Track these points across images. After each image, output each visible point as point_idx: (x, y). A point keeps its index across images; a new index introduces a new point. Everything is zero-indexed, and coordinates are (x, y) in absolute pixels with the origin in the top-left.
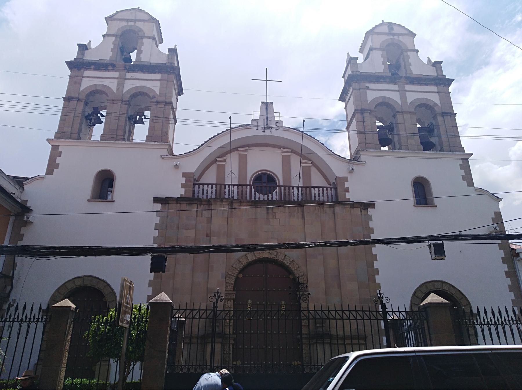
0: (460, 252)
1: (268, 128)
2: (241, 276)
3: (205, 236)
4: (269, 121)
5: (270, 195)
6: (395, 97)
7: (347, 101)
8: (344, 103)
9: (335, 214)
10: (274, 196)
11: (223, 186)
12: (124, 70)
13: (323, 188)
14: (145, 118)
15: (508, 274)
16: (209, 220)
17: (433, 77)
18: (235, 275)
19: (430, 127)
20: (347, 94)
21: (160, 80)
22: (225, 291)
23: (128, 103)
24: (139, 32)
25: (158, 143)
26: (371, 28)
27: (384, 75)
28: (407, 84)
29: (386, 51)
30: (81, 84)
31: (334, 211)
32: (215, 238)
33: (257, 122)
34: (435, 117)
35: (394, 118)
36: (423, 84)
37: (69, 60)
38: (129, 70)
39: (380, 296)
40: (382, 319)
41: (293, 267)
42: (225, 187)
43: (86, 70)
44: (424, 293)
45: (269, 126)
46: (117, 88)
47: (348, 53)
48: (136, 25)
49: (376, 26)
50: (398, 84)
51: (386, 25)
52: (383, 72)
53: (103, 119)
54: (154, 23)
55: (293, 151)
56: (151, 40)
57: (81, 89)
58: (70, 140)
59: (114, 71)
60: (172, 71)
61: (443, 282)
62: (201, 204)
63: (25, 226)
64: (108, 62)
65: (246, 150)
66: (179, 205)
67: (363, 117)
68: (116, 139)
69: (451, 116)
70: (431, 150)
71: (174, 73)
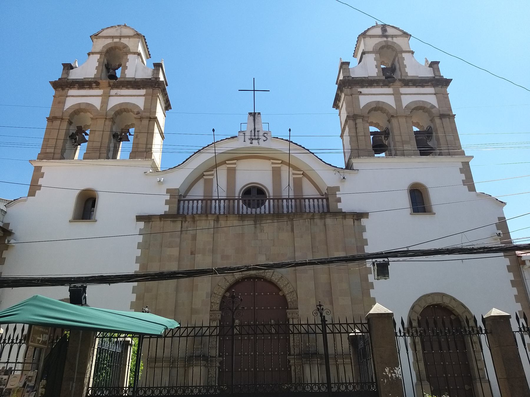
0: (462, 262)
1: (255, 139)
2: (228, 294)
3: (190, 253)
4: (256, 132)
5: (258, 209)
6: (390, 101)
7: (340, 107)
8: (338, 110)
9: (326, 225)
10: (263, 210)
11: (209, 202)
12: (109, 87)
13: (313, 199)
14: (130, 135)
15: (514, 283)
16: (194, 238)
17: (430, 78)
18: (221, 294)
19: (428, 130)
20: (339, 101)
21: (144, 96)
22: (210, 311)
23: (113, 120)
24: (124, 48)
25: (142, 160)
26: (364, 31)
27: (377, 78)
28: (402, 87)
29: (379, 54)
30: (65, 103)
31: (325, 223)
32: (200, 255)
33: (244, 134)
34: (432, 120)
35: (389, 123)
36: (420, 86)
38: (114, 87)
39: (320, 308)
40: (322, 332)
41: (282, 284)
42: (211, 203)
43: (70, 89)
44: (423, 306)
45: (257, 137)
46: (101, 105)
47: (341, 59)
48: (122, 42)
49: (369, 29)
50: (392, 88)
51: (379, 27)
52: (376, 76)
53: (87, 138)
54: (140, 38)
55: (283, 162)
56: (136, 55)
57: (65, 109)
58: (52, 161)
59: (98, 88)
60: (156, 86)
61: (443, 295)
62: (185, 221)
63: (7, 250)
64: (92, 80)
65: (235, 164)
66: (162, 222)
67: (356, 124)
68: (99, 158)
69: (449, 118)
70: (431, 154)
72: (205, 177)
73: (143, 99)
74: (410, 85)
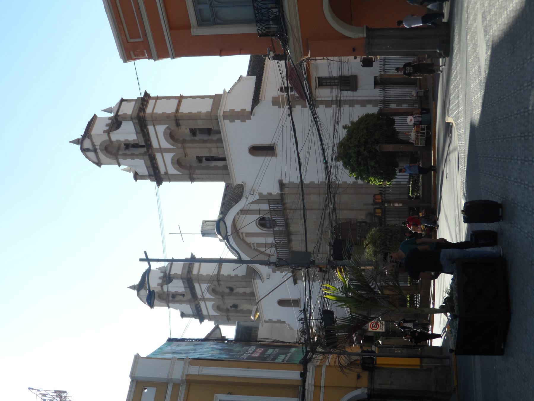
12: (197, 300)
26: (94, 165)
37: (200, 324)
49: (90, 160)
52: (143, 160)
58: (261, 319)
60: (190, 280)
71: (191, 278)
72: (256, 248)
73: (201, 284)
74: (149, 143)
